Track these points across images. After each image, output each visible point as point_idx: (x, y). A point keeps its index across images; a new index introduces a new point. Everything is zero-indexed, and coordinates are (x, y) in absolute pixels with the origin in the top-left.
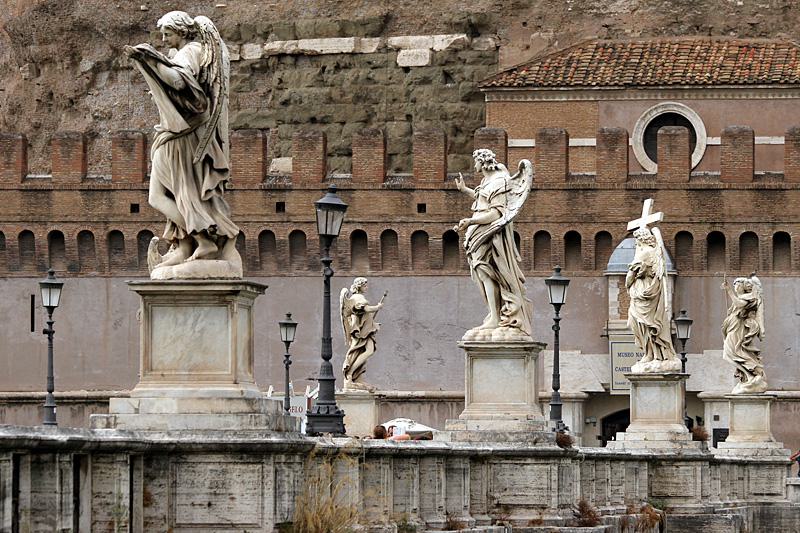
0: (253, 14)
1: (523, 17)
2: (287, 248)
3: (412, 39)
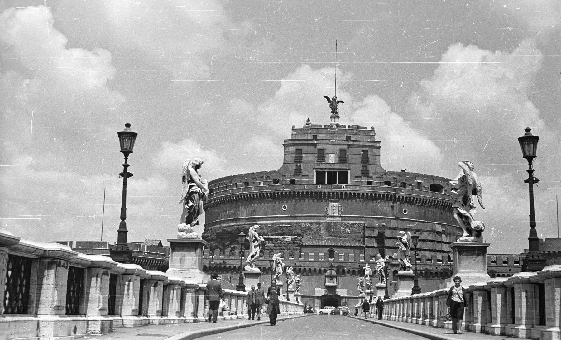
1: (306, 233)
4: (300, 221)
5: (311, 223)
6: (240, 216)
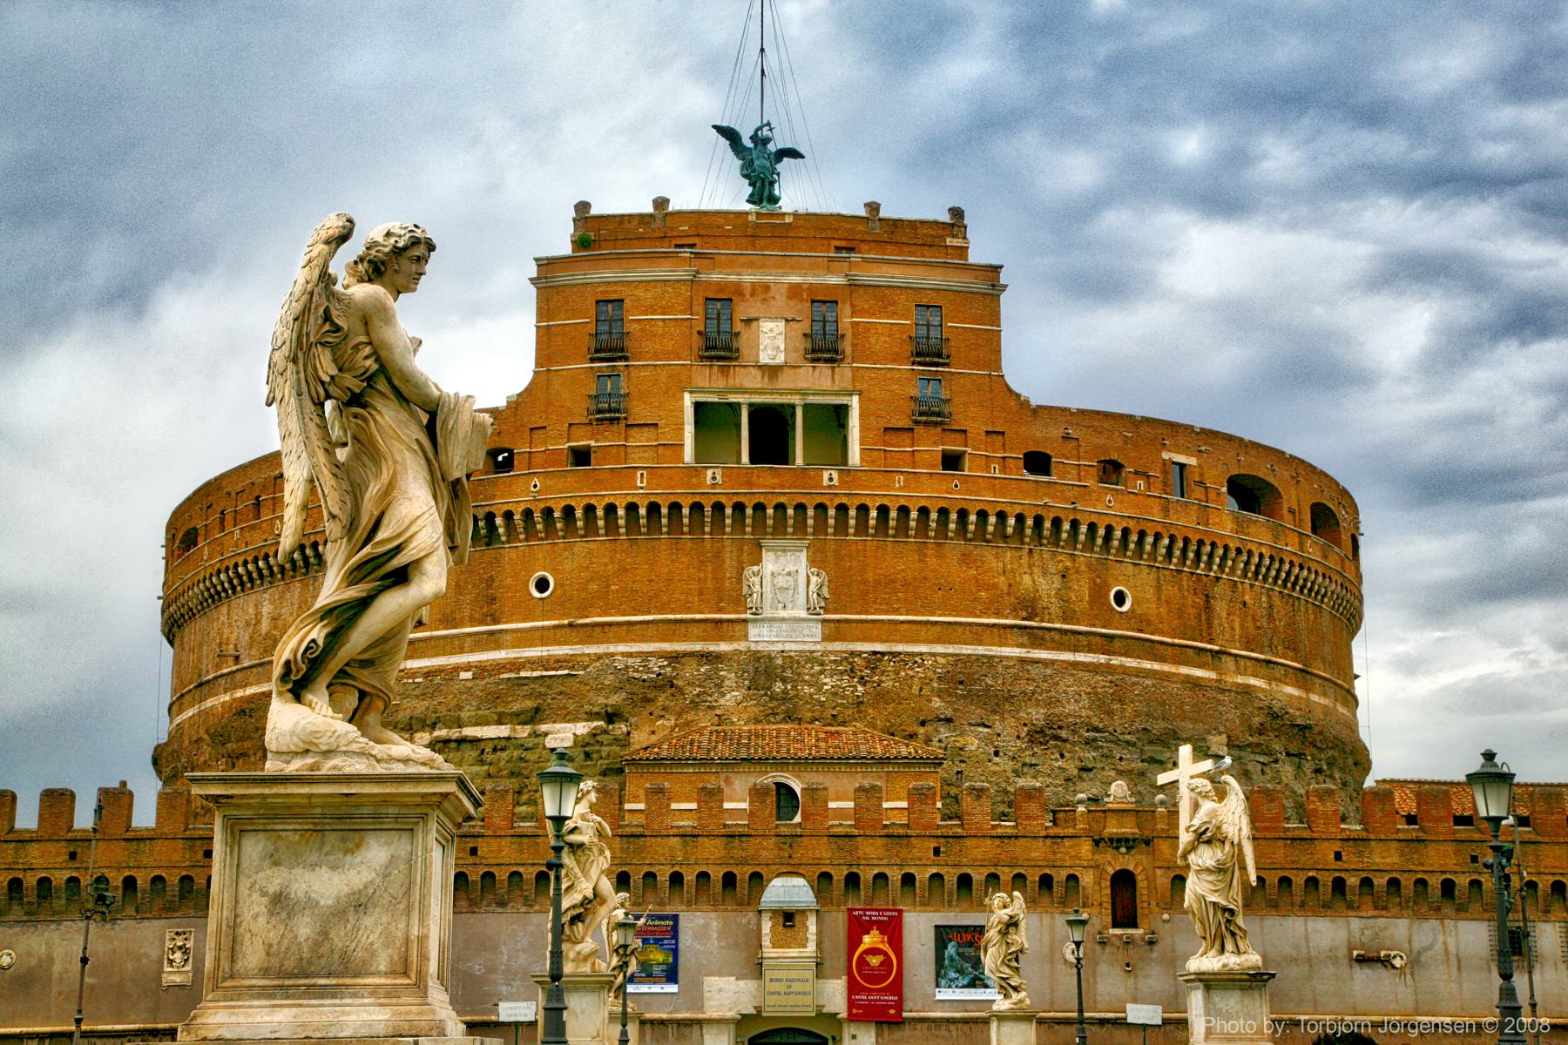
0: (423, 708)
1: (650, 708)
2: (479, 888)
3: (558, 726)
4: (622, 648)
5: (675, 658)
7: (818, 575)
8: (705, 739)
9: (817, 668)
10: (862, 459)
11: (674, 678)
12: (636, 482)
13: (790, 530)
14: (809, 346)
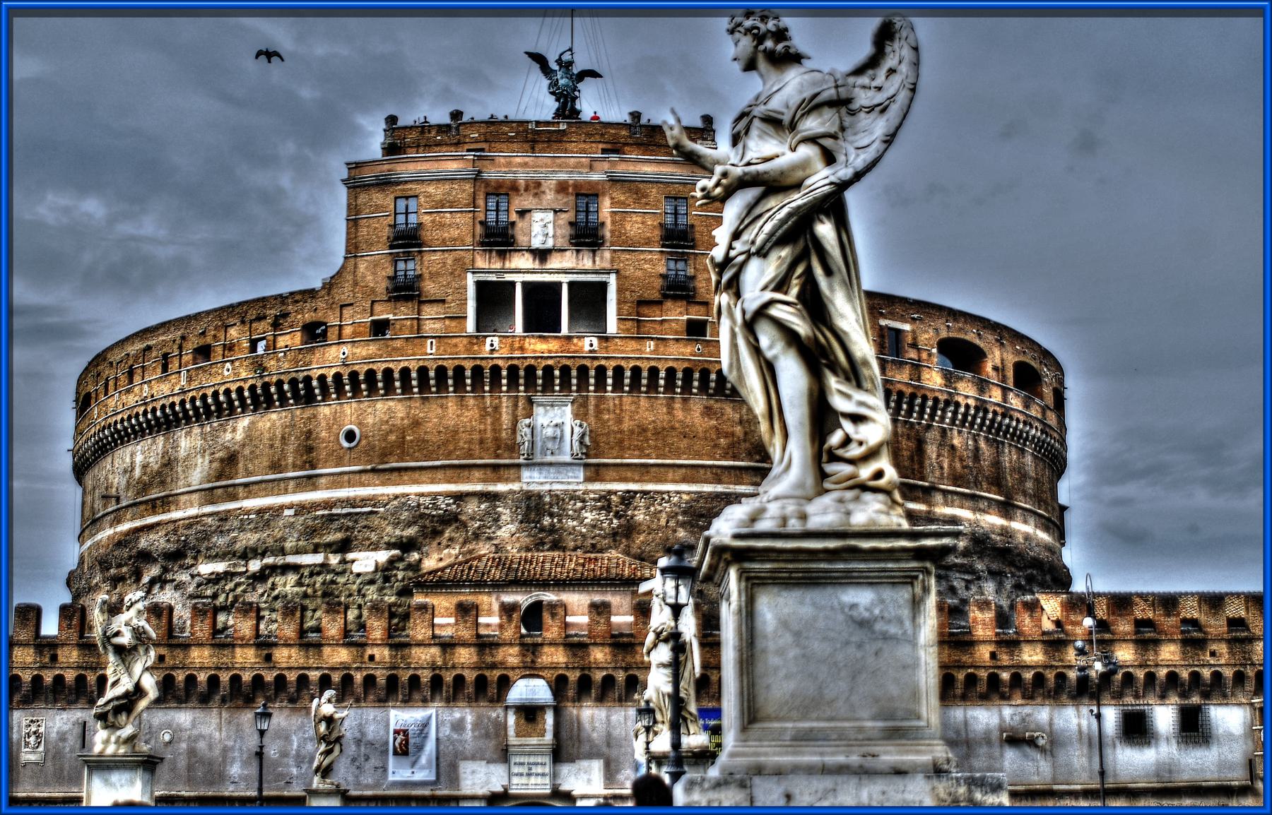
5: (459, 497)
6: (181, 483)
7: (581, 426)
8: (482, 565)
9: (579, 505)
10: (619, 328)
11: (459, 513)
12: (426, 348)
13: (557, 388)
14: (573, 232)
